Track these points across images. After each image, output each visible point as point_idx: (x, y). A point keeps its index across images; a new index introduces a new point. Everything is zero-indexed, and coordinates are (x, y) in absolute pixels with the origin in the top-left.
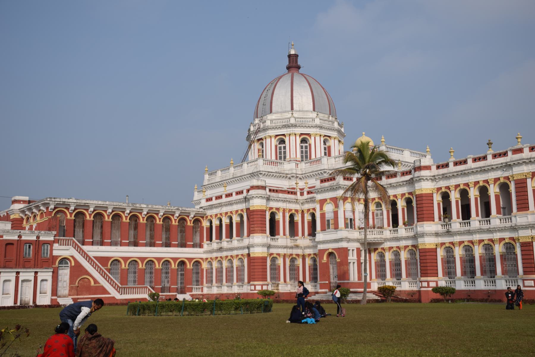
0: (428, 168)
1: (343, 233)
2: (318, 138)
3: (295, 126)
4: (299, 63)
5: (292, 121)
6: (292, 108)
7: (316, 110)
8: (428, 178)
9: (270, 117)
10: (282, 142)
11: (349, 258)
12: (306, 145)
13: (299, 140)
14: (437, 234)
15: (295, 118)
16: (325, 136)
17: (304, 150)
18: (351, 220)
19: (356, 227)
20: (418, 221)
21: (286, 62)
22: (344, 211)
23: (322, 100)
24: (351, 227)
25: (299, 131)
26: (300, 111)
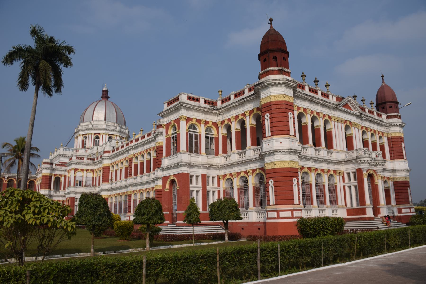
0: (109, 152)
1: (72, 189)
2: (104, 136)
3: (91, 129)
4: (109, 95)
5: (90, 126)
6: (93, 120)
7: (106, 120)
8: (107, 158)
9: (82, 124)
10: (86, 138)
11: (75, 203)
12: (99, 139)
13: (93, 137)
14: (108, 190)
15: (93, 125)
16: (109, 134)
17: (97, 142)
18: (80, 182)
19: (83, 186)
20: (103, 182)
21: (101, 94)
22: (75, 177)
23: (113, 114)
24: (80, 185)
25: (93, 132)
26: (97, 121)
